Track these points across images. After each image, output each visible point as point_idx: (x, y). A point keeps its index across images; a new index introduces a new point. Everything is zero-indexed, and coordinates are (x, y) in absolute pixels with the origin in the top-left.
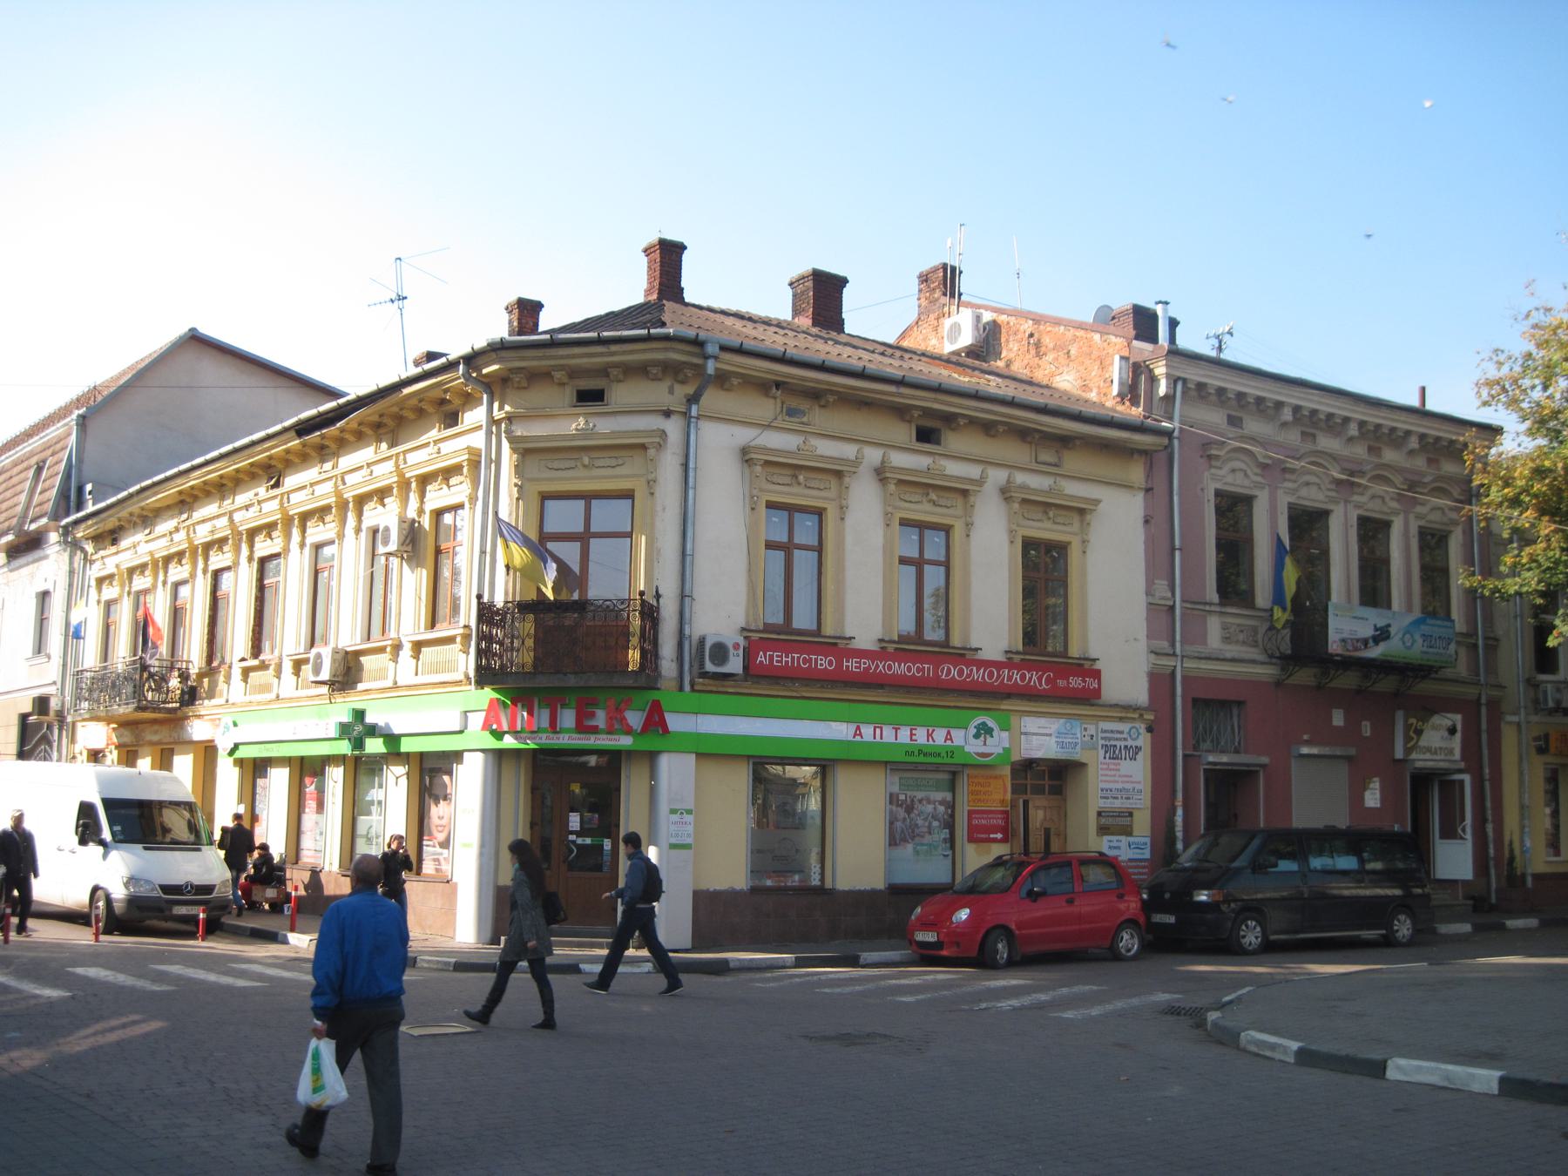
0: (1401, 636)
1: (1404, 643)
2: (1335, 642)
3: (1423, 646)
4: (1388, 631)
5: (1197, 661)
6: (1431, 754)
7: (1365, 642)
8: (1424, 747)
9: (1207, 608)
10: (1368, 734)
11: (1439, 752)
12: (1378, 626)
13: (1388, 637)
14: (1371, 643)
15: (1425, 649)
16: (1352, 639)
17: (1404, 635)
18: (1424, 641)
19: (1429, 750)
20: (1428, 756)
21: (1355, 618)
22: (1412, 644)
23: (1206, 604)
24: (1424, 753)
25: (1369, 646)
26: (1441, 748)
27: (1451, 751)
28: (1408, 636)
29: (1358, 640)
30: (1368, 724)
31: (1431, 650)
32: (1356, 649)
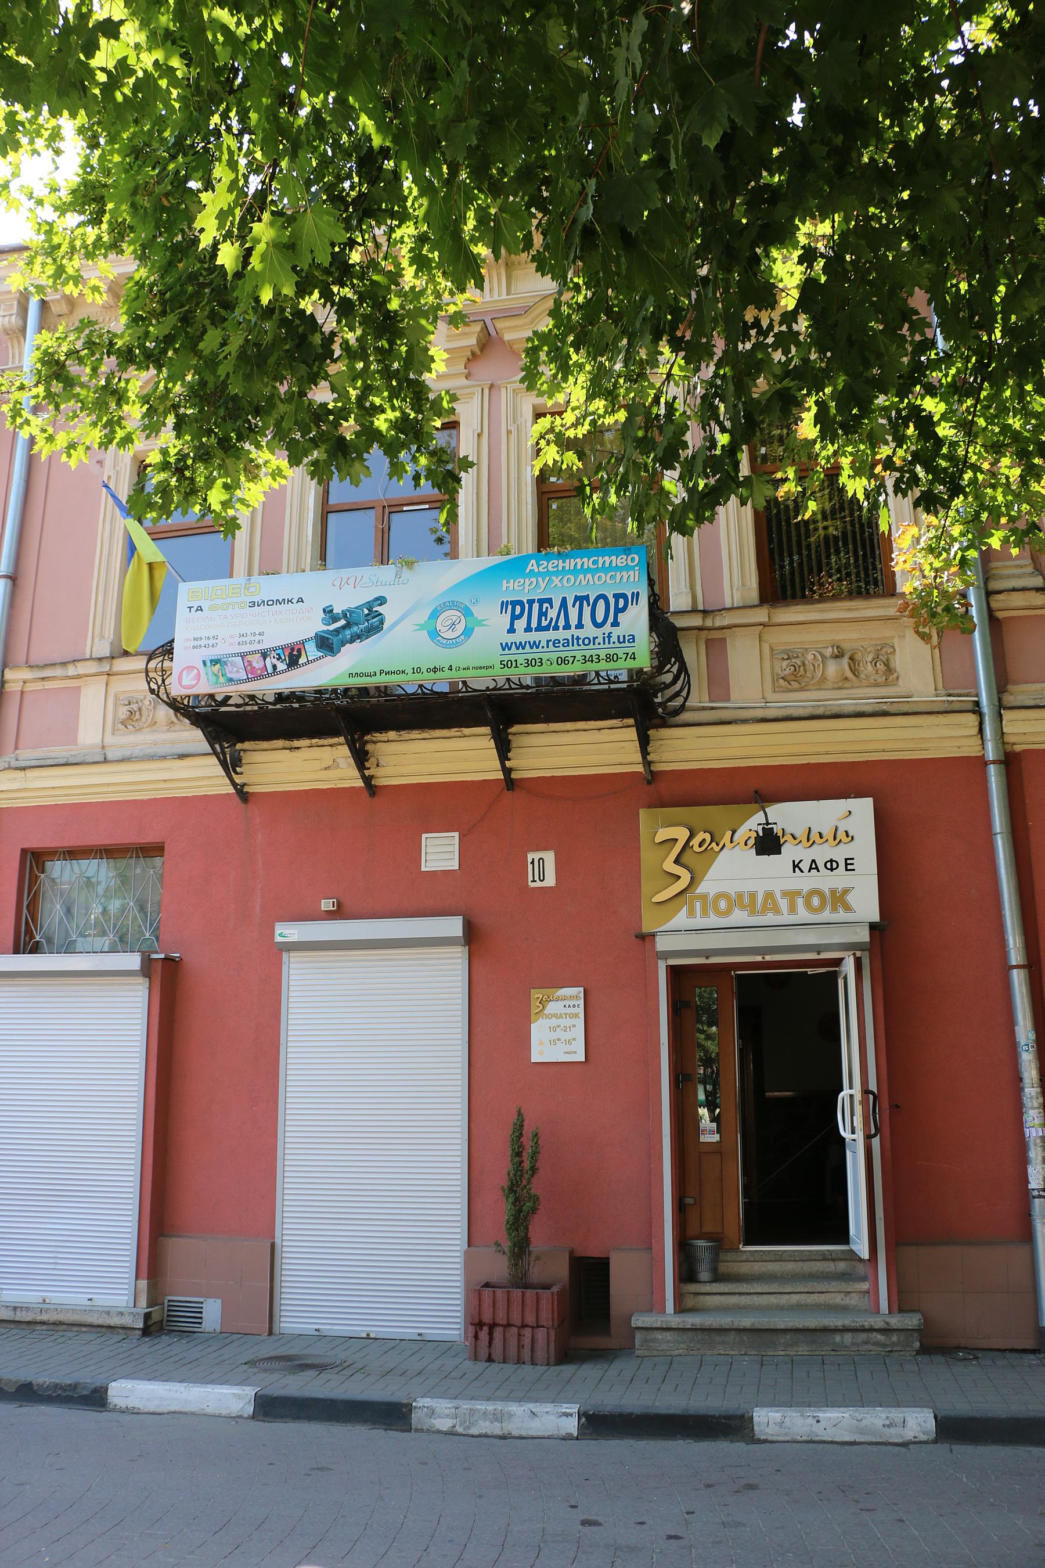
0: (422, 616)
1: (434, 634)
2: (190, 668)
3: (512, 630)
4: (373, 614)
5: (20, 774)
6: (753, 912)
7: (293, 657)
8: (721, 895)
9: (71, 671)
10: (550, 881)
11: (783, 904)
12: (337, 610)
13: (377, 629)
14: (312, 650)
15: (520, 636)
16: (243, 656)
17: (435, 615)
18: (514, 617)
19: (738, 901)
20: (740, 917)
21: (253, 604)
22: (468, 632)
23: (64, 664)
24: (728, 912)
25: (301, 661)
26: (791, 895)
27: (839, 899)
28: (452, 614)
29: (264, 655)
30: (549, 857)
31: (543, 637)
32: (263, 675)
